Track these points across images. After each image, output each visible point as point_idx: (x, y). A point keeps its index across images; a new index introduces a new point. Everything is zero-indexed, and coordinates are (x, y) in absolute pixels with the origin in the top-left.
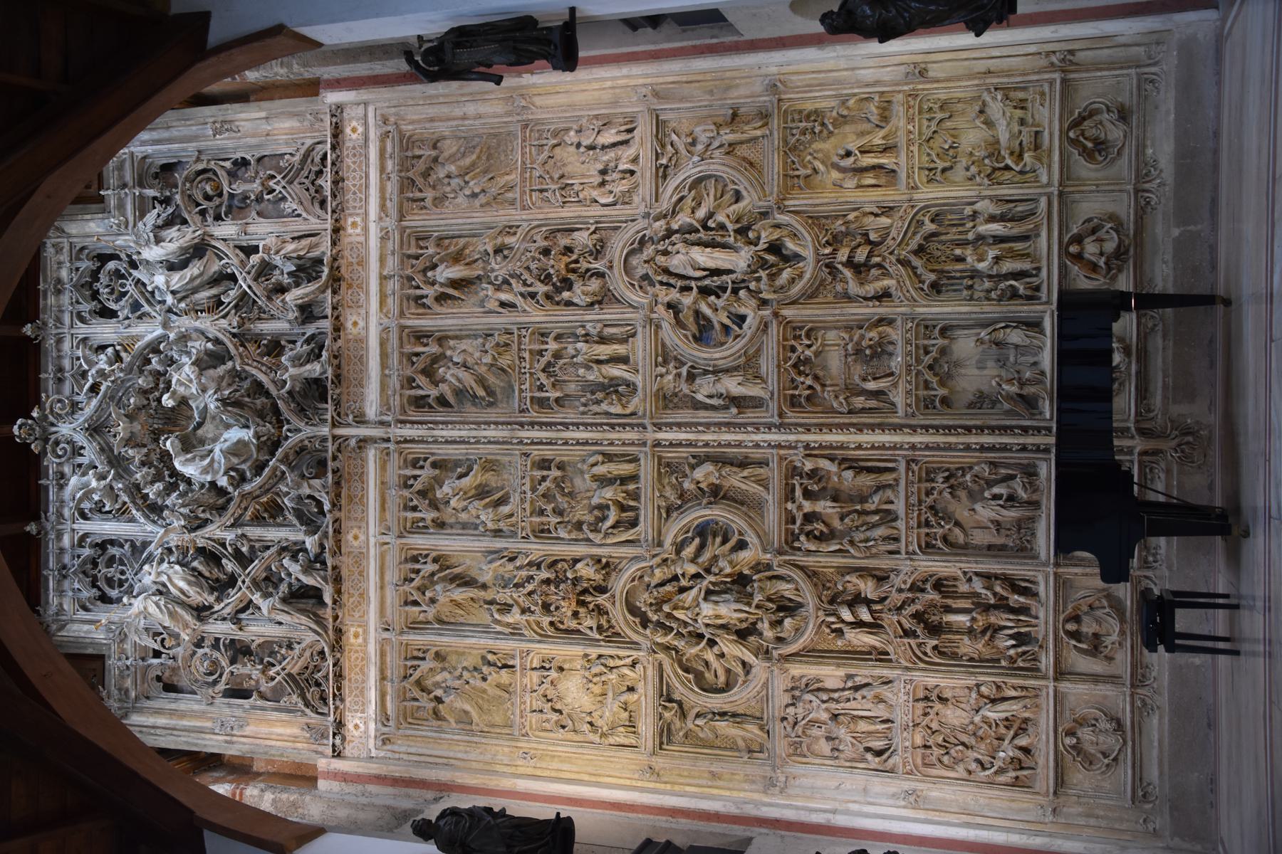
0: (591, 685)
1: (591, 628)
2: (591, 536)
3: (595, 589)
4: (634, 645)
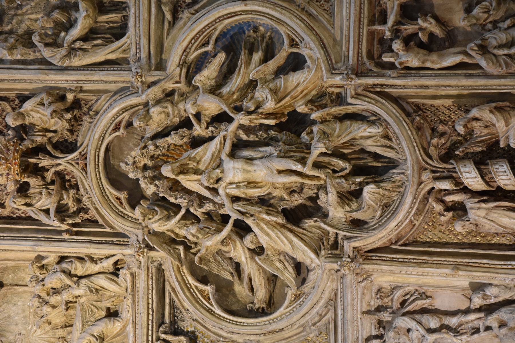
0: (46, 309)
1: (47, 212)
2: (47, 53)
3: (56, 146)
4: (119, 238)
